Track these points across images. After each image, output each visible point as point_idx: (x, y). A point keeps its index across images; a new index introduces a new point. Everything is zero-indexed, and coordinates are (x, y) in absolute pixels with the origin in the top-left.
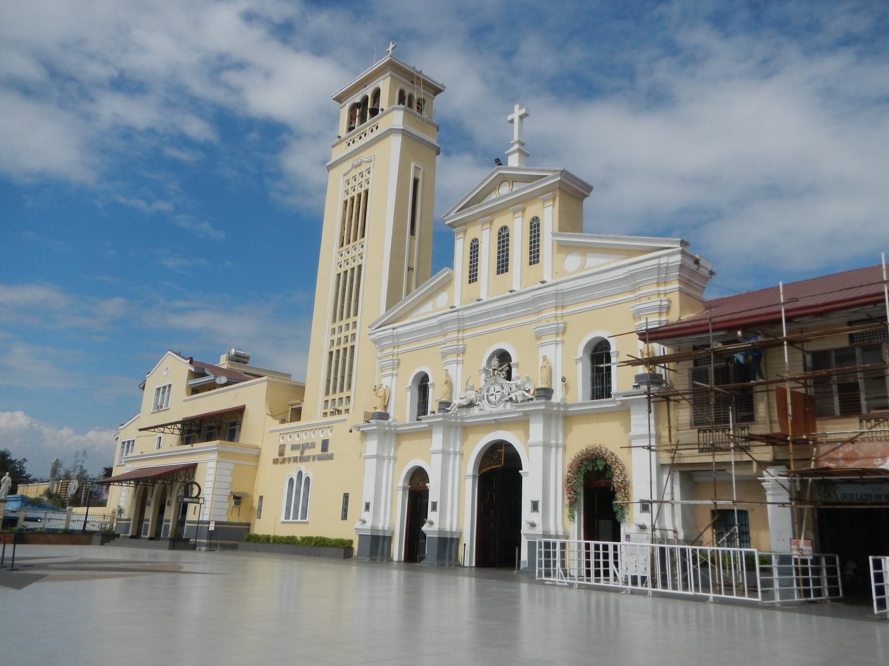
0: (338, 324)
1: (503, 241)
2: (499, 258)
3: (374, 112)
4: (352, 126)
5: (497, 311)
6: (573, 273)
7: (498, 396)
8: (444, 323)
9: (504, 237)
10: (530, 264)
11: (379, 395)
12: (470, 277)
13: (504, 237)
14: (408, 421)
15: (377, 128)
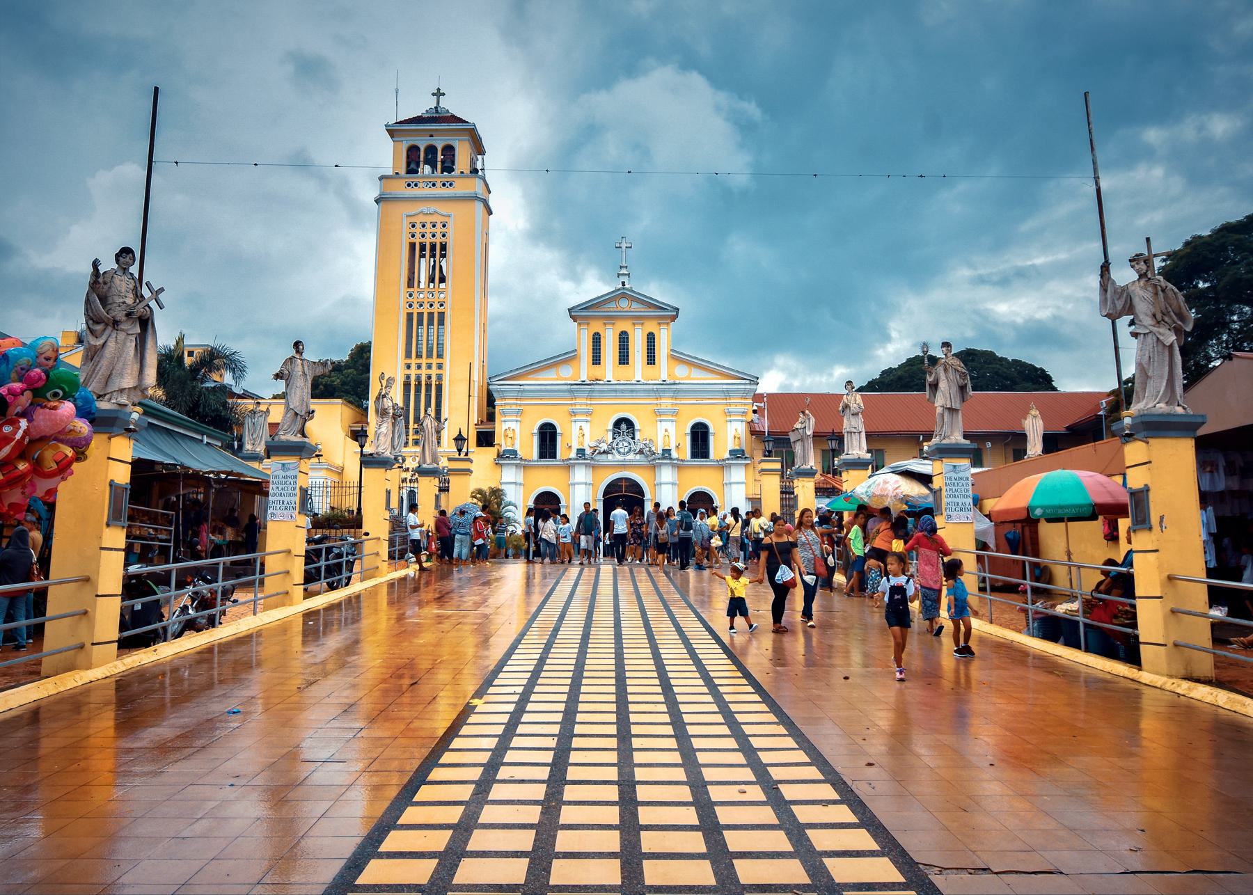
0: (414, 361)
1: (624, 342)
2: (620, 352)
3: (448, 168)
4: (413, 166)
5: (623, 391)
6: (682, 379)
7: (627, 449)
8: (577, 391)
9: (624, 339)
10: (648, 364)
11: (510, 436)
12: (593, 360)
13: (624, 339)
14: (536, 459)
15: (451, 185)
